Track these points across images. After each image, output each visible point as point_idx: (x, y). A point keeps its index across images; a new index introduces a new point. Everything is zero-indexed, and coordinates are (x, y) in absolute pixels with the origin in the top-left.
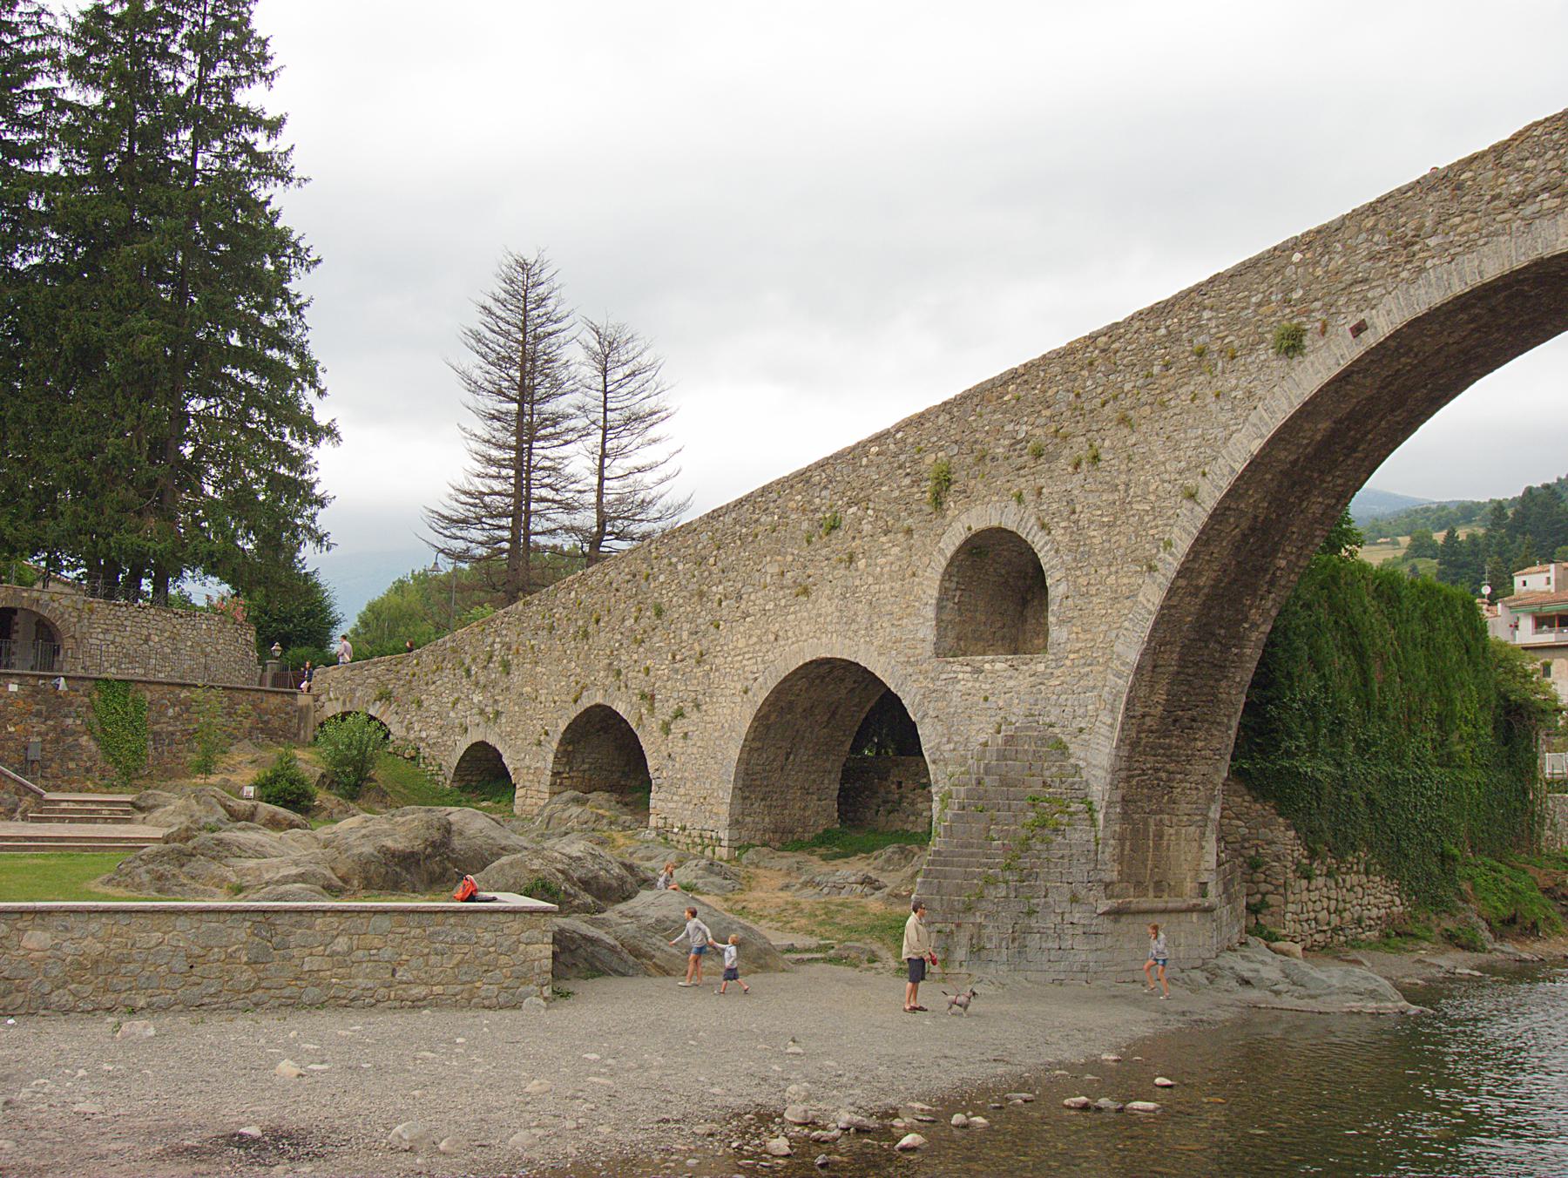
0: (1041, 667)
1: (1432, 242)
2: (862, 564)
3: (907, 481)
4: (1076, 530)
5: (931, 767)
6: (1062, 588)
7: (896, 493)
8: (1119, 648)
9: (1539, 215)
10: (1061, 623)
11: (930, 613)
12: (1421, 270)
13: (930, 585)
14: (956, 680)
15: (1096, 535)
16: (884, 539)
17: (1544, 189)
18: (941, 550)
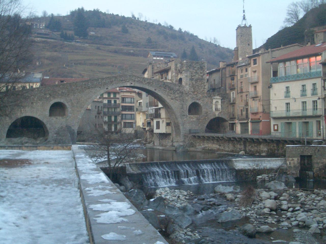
0: (67, 118)
1: (114, 82)
2: (35, 104)
3: (43, 94)
4: (72, 104)
5: (49, 130)
6: (70, 110)
7: (41, 96)
8: (78, 117)
9: (123, 82)
10: (70, 113)
11: (48, 111)
12: (113, 84)
13: (48, 108)
14: (53, 119)
15: (75, 104)
16: (39, 101)
17: (124, 80)
18: (50, 104)
